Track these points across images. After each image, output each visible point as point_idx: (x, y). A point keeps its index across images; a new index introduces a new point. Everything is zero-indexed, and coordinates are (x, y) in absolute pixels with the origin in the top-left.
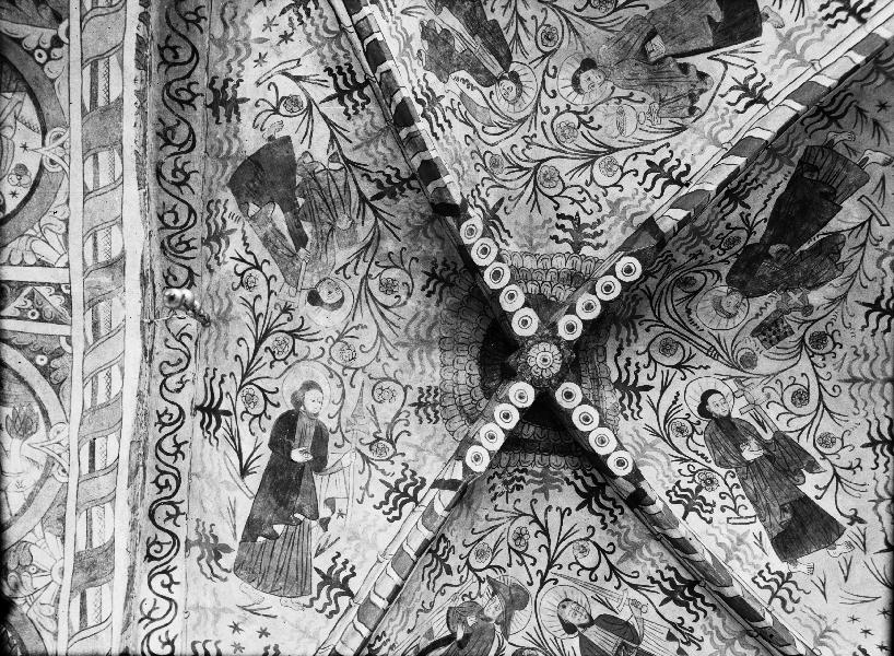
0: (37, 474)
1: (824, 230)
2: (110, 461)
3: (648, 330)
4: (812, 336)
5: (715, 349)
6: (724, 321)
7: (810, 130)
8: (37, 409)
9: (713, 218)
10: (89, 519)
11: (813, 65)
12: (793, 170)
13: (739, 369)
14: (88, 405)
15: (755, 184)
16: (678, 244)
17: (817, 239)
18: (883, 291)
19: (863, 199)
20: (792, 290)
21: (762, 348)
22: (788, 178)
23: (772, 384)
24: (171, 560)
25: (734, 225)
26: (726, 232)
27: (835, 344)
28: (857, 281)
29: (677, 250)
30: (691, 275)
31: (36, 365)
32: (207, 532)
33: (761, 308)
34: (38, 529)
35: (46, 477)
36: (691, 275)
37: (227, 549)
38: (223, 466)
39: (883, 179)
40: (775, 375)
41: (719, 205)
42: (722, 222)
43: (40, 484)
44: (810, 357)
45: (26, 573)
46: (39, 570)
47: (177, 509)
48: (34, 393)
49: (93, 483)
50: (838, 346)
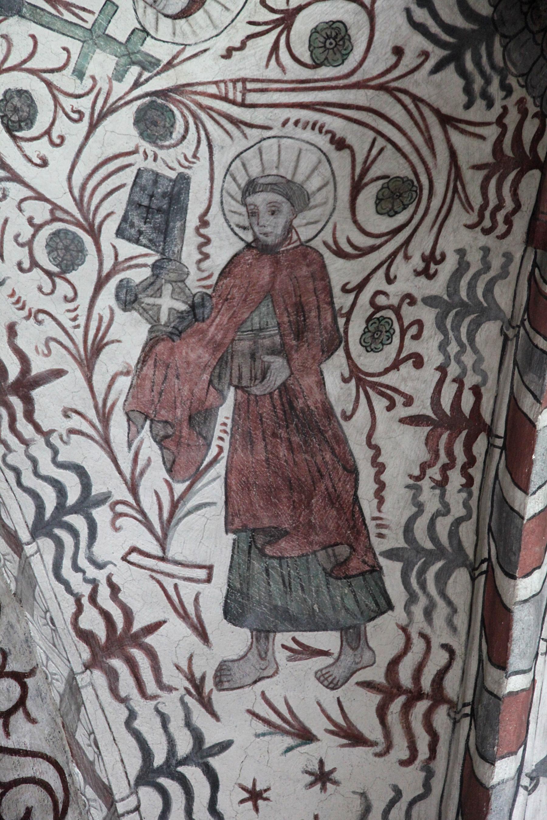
1: (220, 468)
3: (398, 51)
4: (81, 250)
5: (233, 102)
6: (255, 170)
7: (418, 645)
9: (469, 359)
11: (532, 779)
12: (379, 546)
13: (163, 93)
15: (435, 472)
16: (496, 263)
17: (215, 442)
18: (37, 428)
19: (202, 574)
20: (181, 315)
21: (150, 164)
22: (371, 525)
23: (85, 104)
25: (407, 368)
26: (411, 346)
27: (34, 264)
28: (92, 414)
29: (486, 250)
30: (402, 218)
33: (208, 241)
36: (402, 218)
39: (203, 635)
40: (93, 127)
41: (476, 391)
42: (439, 359)
44: (55, 207)
50: (26, 265)
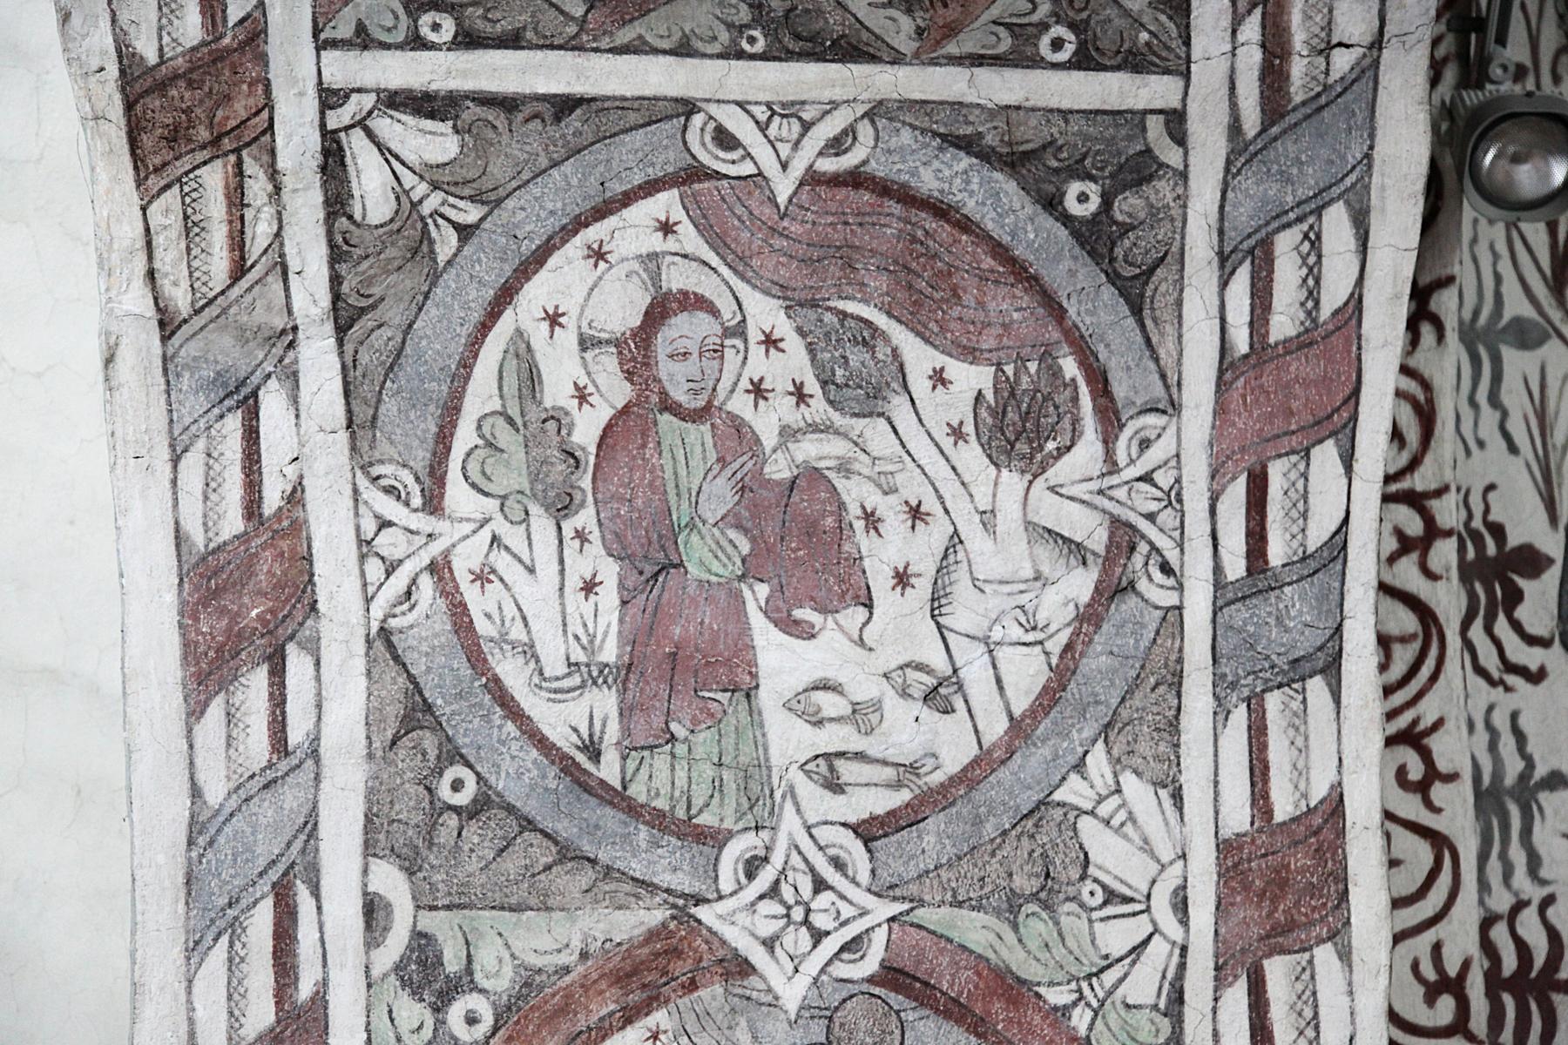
0: (1080, 584)
2: (1319, 531)
8: (1070, 367)
10: (1257, 733)
14: (1241, 341)
24: (1420, 695)
31: (1066, 219)
32: (1477, 523)
34: (1098, 761)
35: (1114, 589)
37: (1531, 561)
38: (1505, 267)
43: (1090, 617)
45: (1071, 907)
46: (1111, 897)
47: (1429, 520)
48: (1057, 311)
49: (1263, 609)
